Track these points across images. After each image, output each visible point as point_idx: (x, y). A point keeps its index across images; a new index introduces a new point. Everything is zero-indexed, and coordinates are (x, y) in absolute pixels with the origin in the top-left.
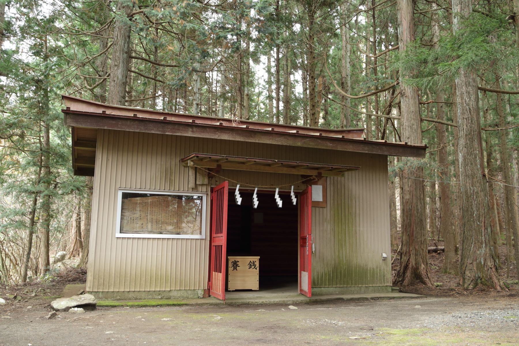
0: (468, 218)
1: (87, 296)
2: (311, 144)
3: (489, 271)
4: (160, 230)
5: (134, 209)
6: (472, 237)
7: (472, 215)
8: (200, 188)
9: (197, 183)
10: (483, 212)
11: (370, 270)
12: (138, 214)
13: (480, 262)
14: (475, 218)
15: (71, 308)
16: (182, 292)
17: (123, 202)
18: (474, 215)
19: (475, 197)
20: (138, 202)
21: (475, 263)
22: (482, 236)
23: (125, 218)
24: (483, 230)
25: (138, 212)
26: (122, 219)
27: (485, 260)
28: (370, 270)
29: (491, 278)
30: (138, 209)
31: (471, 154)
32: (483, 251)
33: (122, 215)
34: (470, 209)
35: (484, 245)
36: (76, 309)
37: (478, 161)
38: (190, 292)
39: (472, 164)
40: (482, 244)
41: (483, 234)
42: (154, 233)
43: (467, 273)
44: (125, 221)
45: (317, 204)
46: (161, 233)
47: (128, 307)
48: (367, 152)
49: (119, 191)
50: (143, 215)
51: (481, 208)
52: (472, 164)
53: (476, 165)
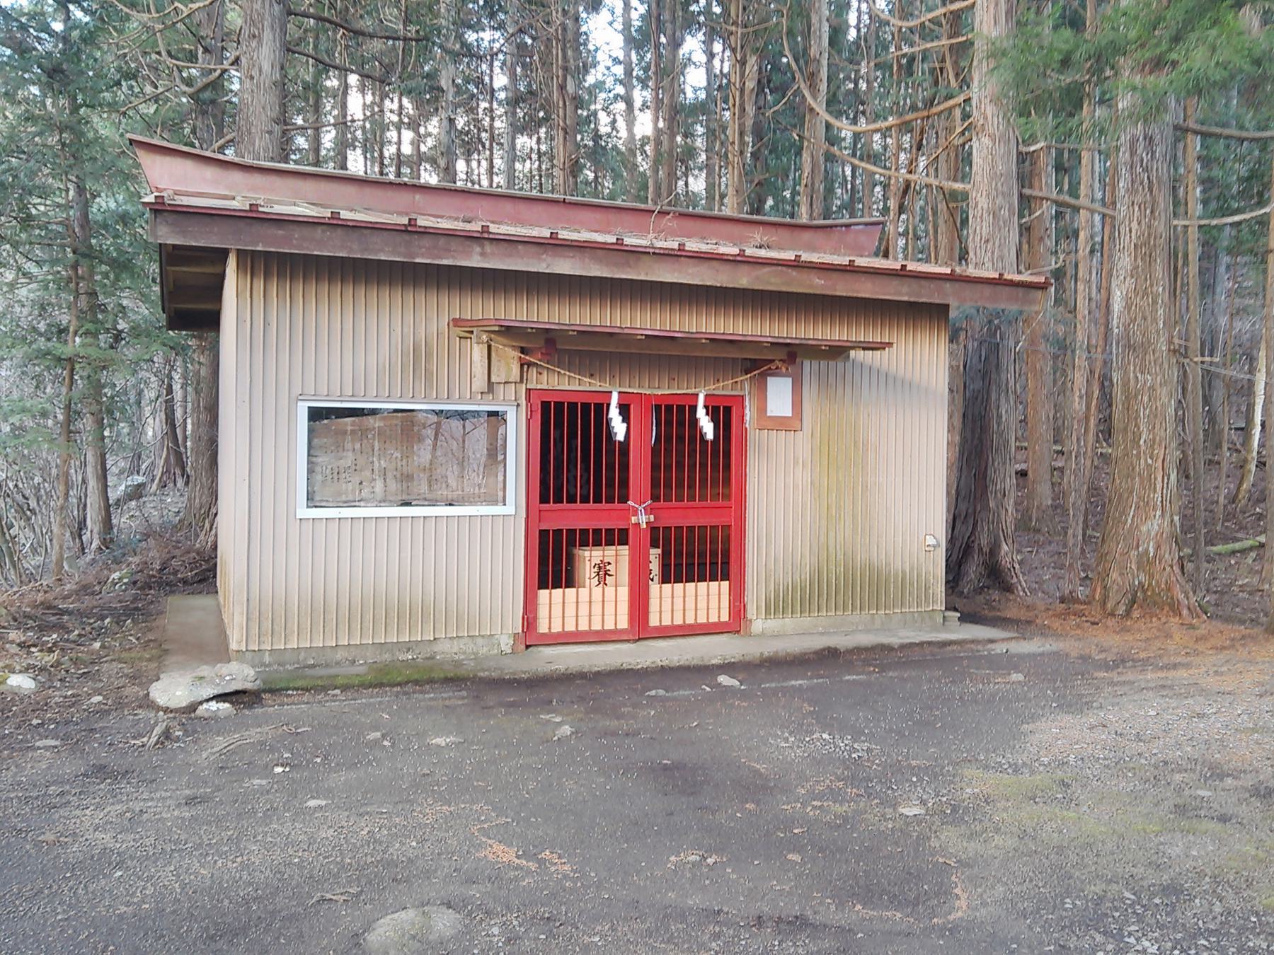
0: (1126, 447)
1: (234, 667)
2: (773, 280)
3: (1166, 574)
4: (405, 497)
5: (340, 447)
6: (1132, 492)
7: (1136, 442)
8: (500, 390)
9: (494, 379)
10: (1163, 434)
11: (896, 575)
12: (348, 459)
13: (1147, 551)
14: (1143, 448)
15: (201, 703)
16: (462, 641)
17: (311, 431)
18: (1142, 442)
19: (1146, 399)
20: (349, 428)
21: (1133, 553)
22: (1155, 491)
23: (318, 469)
24: (1160, 479)
25: (350, 454)
26: (310, 471)
27: (1158, 547)
28: (896, 575)
29: (1169, 589)
30: (349, 446)
31: (1145, 293)
32: (1156, 527)
33: (309, 462)
34: (1132, 427)
35: (1159, 513)
36: (213, 706)
37: (1161, 312)
38: (480, 641)
39: (1145, 319)
40: (1155, 510)
41: (1159, 486)
42: (392, 504)
43: (1114, 575)
44: (319, 477)
45: (781, 424)
46: (408, 504)
47: (337, 691)
48: (906, 299)
49: (300, 403)
50: (362, 461)
51: (1157, 426)
52: (1145, 319)
53: (1155, 320)
